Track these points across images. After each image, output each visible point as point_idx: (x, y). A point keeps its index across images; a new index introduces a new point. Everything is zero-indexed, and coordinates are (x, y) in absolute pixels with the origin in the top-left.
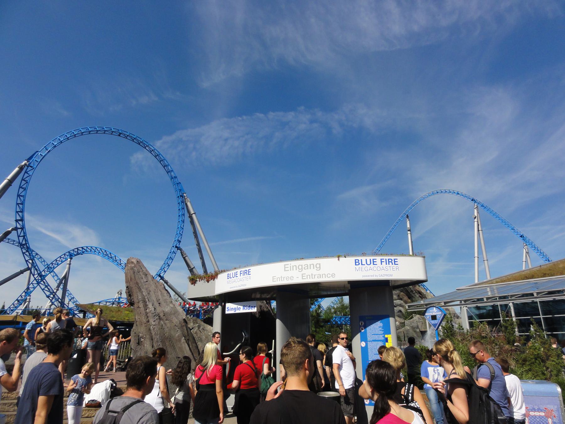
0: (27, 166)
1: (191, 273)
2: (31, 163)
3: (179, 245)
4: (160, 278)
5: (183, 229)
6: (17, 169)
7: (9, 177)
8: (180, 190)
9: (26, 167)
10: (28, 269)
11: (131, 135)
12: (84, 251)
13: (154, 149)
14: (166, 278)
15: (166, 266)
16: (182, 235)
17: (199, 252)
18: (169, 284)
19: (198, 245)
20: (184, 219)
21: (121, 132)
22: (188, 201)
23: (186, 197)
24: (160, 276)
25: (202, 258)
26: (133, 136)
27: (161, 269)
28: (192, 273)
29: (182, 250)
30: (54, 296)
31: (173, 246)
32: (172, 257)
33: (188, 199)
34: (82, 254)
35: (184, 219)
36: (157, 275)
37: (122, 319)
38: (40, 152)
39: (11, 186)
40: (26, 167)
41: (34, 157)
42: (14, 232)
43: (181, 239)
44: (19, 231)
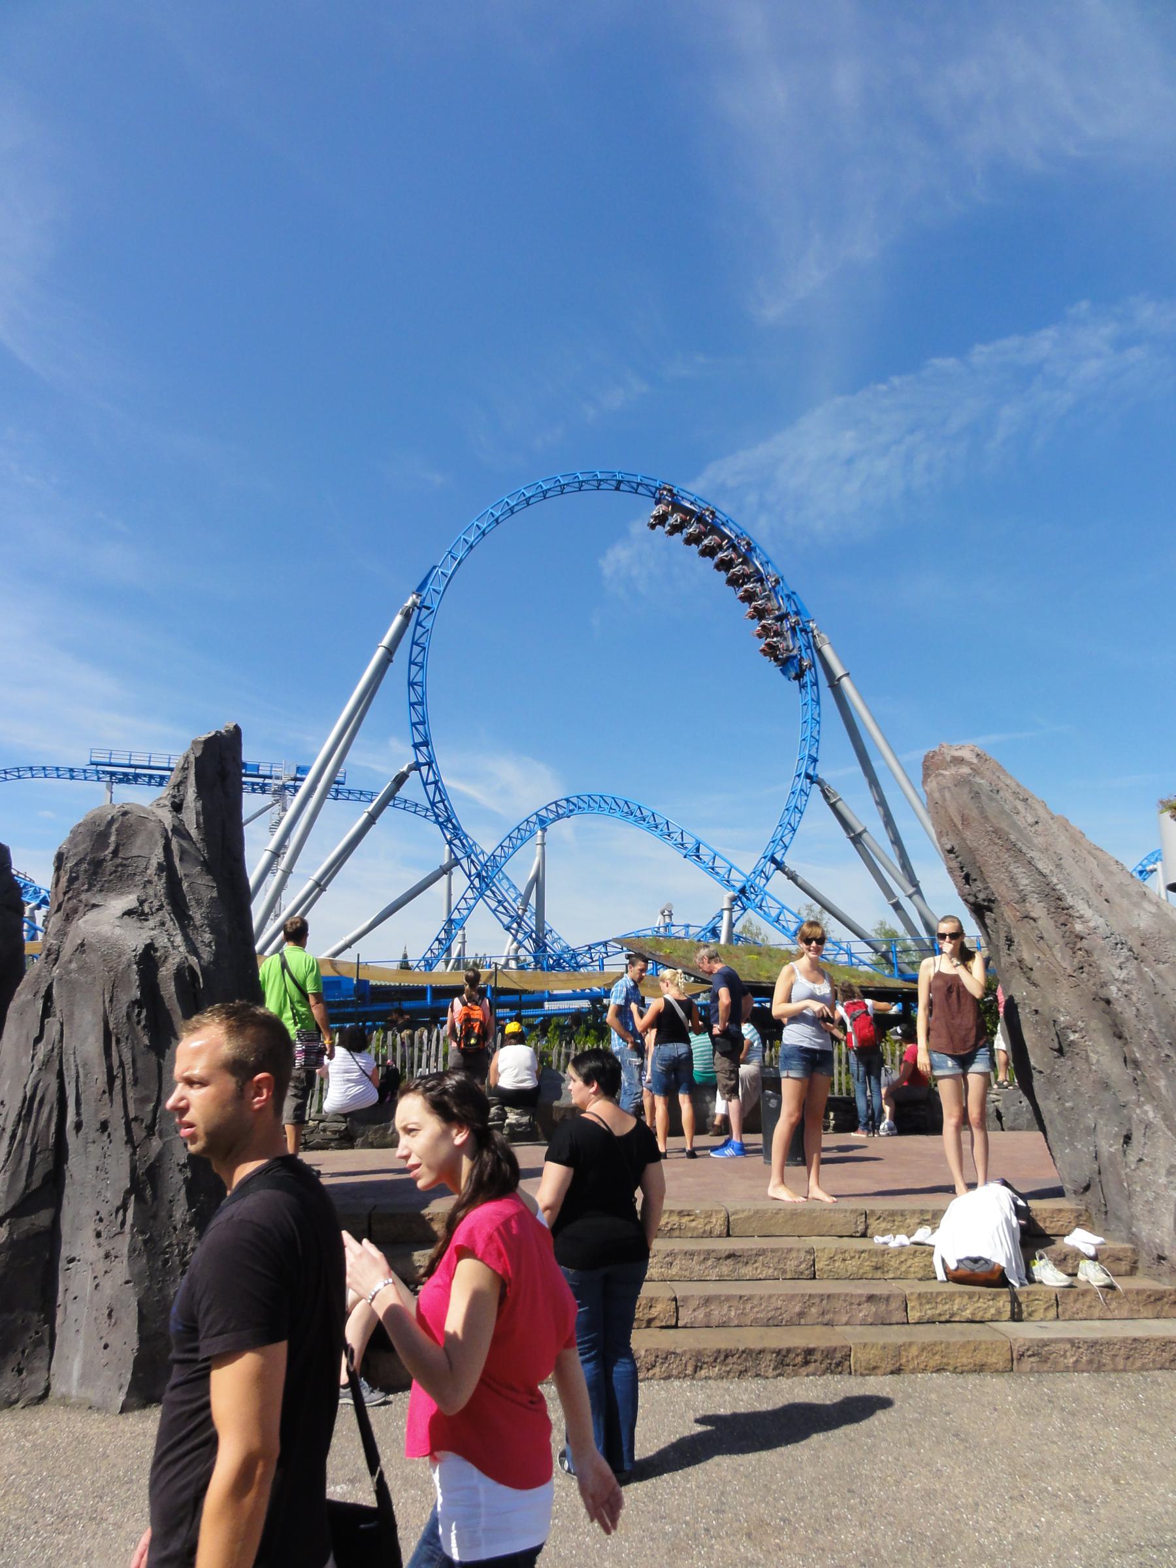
0: (418, 608)
1: (858, 845)
2: (425, 598)
4: (773, 866)
5: (818, 722)
6: (398, 619)
7: (386, 641)
9: (417, 611)
11: (646, 481)
12: (572, 807)
14: (790, 864)
15: (787, 831)
17: (871, 787)
18: (800, 881)
23: (816, 632)
24: (773, 860)
26: (652, 483)
27: (773, 842)
30: (519, 925)
31: (799, 776)
33: (823, 635)
34: (569, 817)
36: (765, 858)
37: (755, 976)
40: (417, 611)
42: (414, 774)
44: (424, 769)
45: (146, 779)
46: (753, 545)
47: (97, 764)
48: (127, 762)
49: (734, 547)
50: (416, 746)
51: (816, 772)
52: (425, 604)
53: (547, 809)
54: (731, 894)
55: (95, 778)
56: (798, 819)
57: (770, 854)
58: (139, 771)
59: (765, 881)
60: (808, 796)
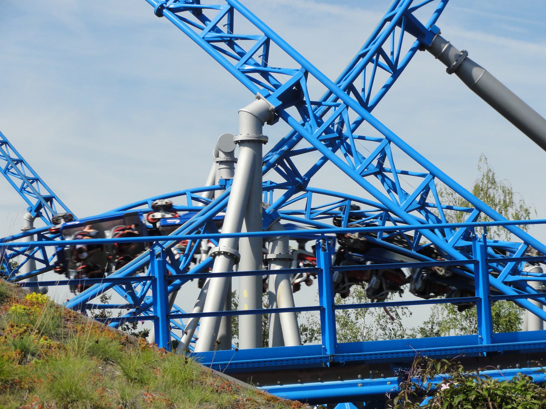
4: (411, 40)
18: (477, 75)
57: (399, 10)
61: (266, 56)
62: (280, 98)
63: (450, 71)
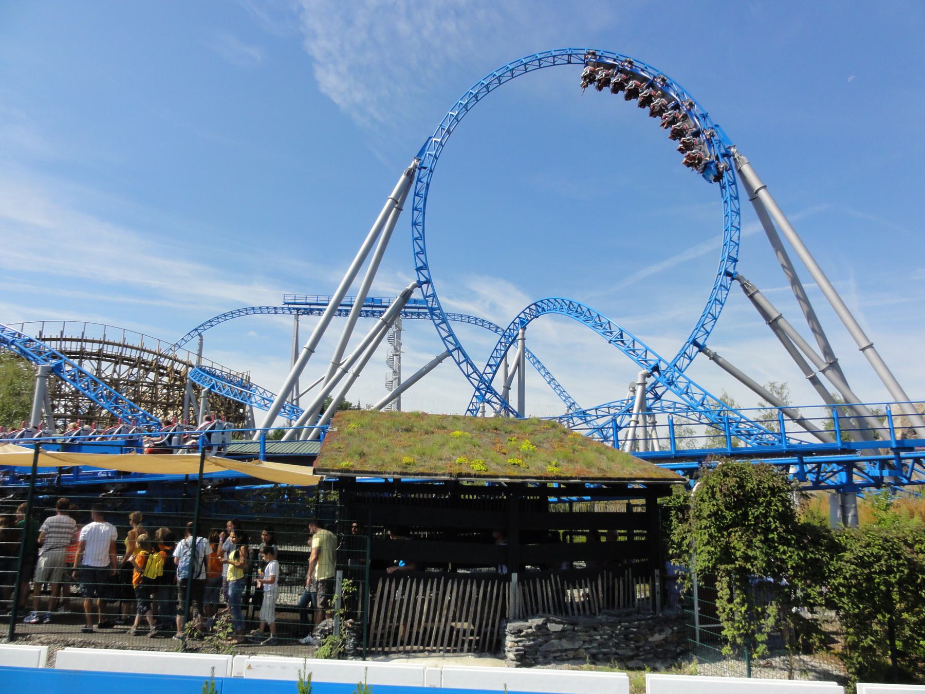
0: (419, 169)
2: (423, 161)
3: (734, 268)
4: (696, 349)
6: (403, 177)
8: (720, 142)
10: (449, 353)
13: (646, 68)
14: (712, 348)
16: (737, 244)
18: (720, 360)
19: (788, 266)
20: (738, 207)
21: (570, 53)
22: (743, 162)
23: (736, 156)
24: (695, 343)
25: (803, 298)
28: (779, 331)
29: (745, 280)
32: (719, 297)
33: (742, 157)
35: (738, 207)
38: (434, 137)
39: (402, 210)
41: (426, 149)
43: (737, 254)
45: (317, 312)
46: (668, 81)
47: (289, 304)
48: (304, 301)
49: (651, 85)
50: (418, 269)
51: (736, 270)
52: (424, 165)
53: (524, 313)
54: (645, 371)
55: (289, 312)
56: (718, 310)
57: (691, 339)
58: (312, 307)
59: (688, 361)
60: (728, 290)
61: (646, 356)
62: (652, 369)
63: (710, 359)
